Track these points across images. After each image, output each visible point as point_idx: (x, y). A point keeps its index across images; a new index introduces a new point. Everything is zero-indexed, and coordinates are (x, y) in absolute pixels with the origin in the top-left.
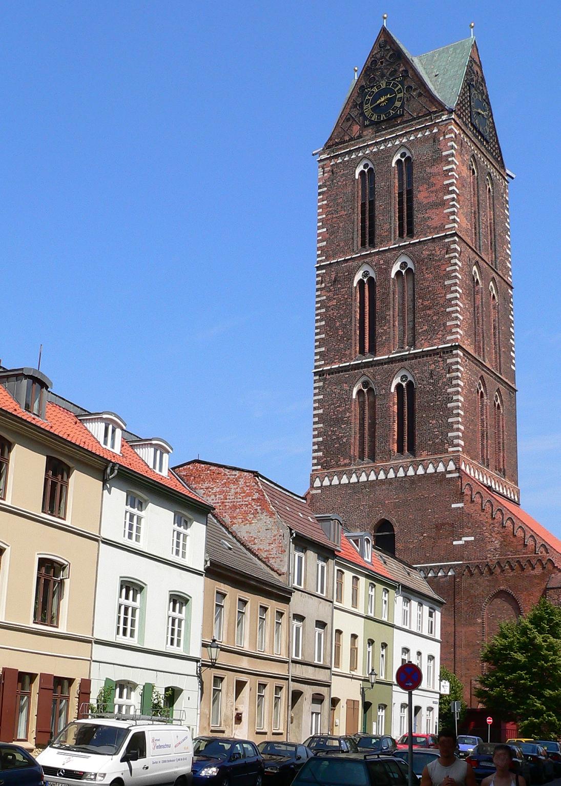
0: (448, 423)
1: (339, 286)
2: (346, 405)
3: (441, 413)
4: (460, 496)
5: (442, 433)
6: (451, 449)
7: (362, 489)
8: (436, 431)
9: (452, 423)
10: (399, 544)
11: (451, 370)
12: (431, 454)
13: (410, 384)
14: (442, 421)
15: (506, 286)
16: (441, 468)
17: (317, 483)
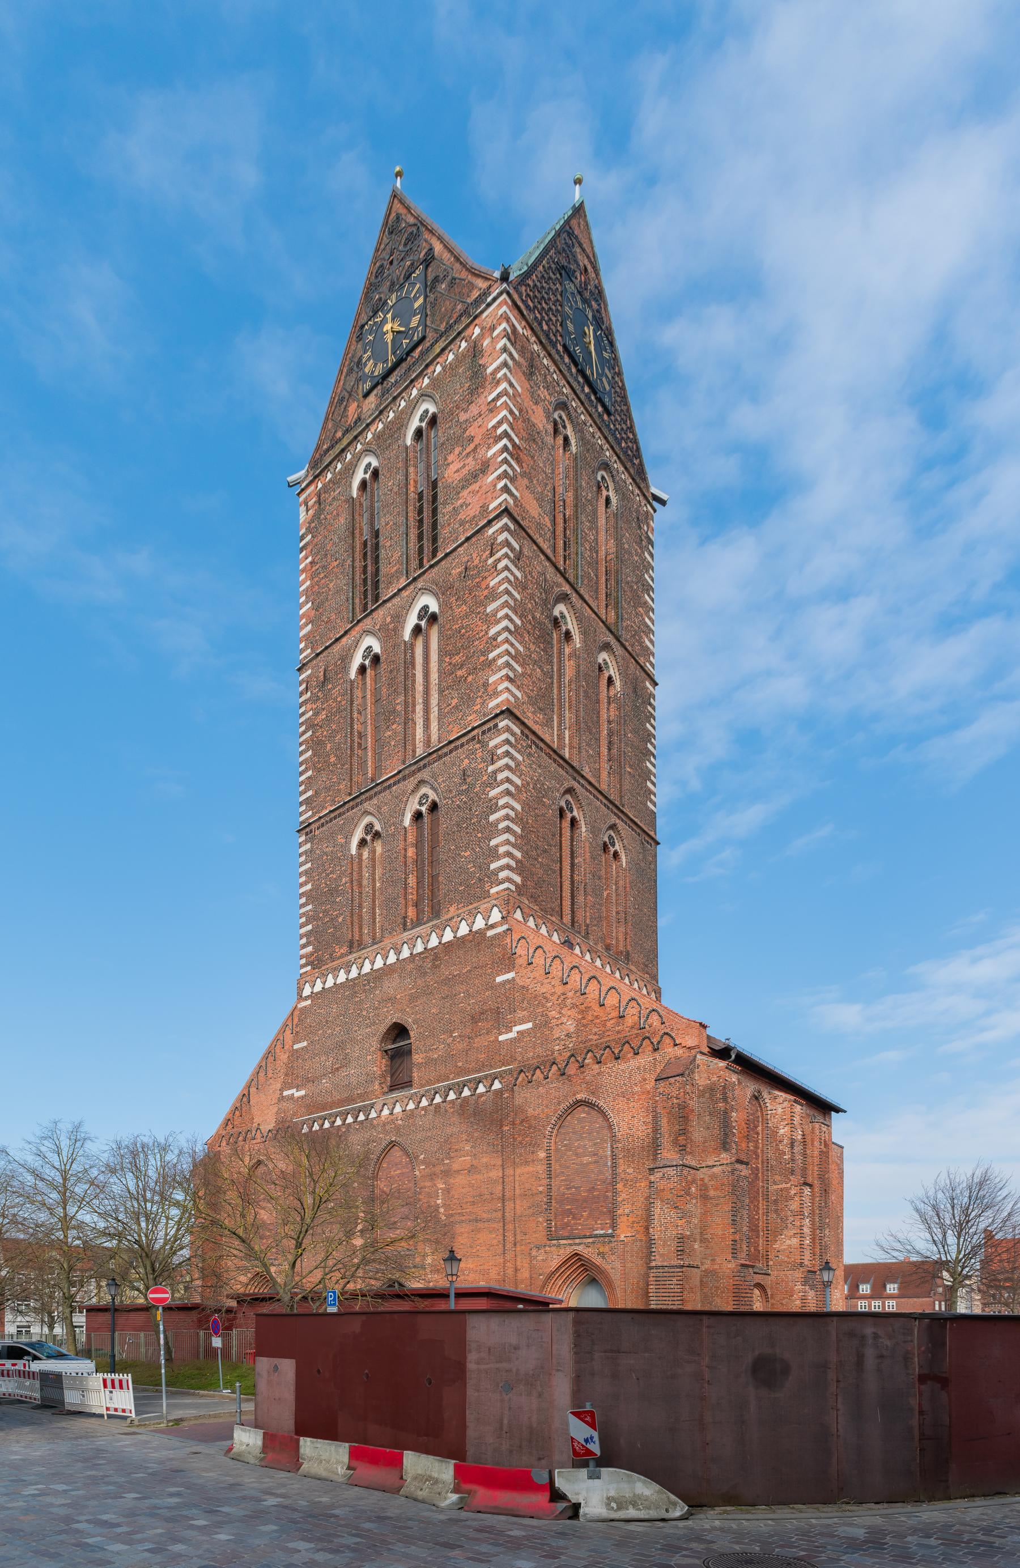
0: (490, 849)
1: (330, 686)
2: (341, 866)
3: (480, 835)
4: (508, 961)
5: (480, 867)
6: (493, 891)
7: (364, 985)
8: (471, 868)
9: (497, 846)
10: (417, 1056)
11: (495, 758)
12: (464, 906)
13: (434, 807)
14: (481, 847)
15: (639, 672)
16: (479, 923)
17: (307, 991)
